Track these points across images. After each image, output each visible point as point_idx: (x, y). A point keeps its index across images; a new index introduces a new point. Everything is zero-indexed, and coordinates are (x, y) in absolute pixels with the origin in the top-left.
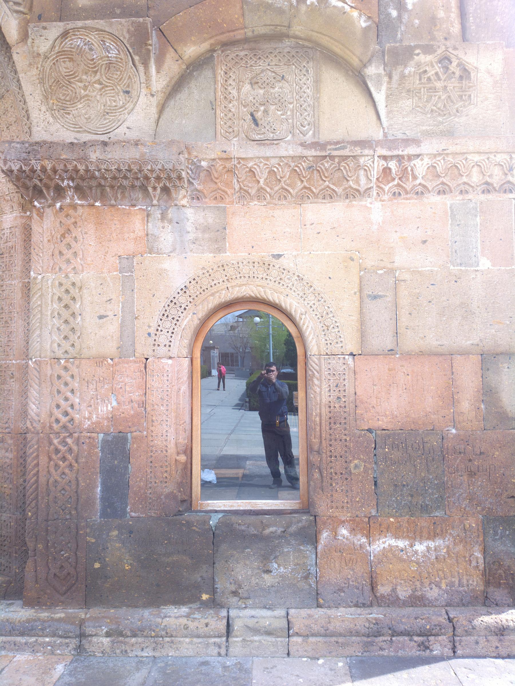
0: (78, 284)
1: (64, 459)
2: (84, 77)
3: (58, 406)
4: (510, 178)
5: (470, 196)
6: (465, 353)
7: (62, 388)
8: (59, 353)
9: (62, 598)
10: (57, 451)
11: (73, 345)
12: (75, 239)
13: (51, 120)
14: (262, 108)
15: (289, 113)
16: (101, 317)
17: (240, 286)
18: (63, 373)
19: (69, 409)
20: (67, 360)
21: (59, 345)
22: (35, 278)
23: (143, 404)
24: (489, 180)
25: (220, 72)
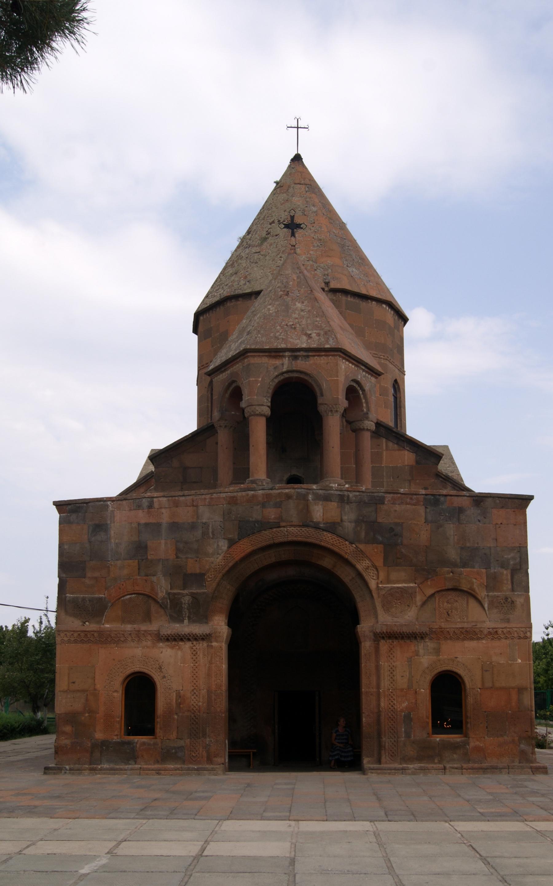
0: (395, 666)
1: (392, 720)
2: (395, 601)
3: (390, 704)
4: (526, 635)
5: (515, 640)
6: (513, 688)
7: (391, 698)
8: (390, 687)
9: (393, 762)
10: (390, 717)
11: (394, 685)
12: (394, 652)
13: (384, 614)
14: (450, 610)
15: (459, 612)
16: (402, 677)
17: (445, 667)
18: (391, 694)
19: (393, 705)
20: (392, 690)
21: (389, 685)
22: (382, 664)
23: (416, 704)
24: (520, 635)
25: (437, 599)
